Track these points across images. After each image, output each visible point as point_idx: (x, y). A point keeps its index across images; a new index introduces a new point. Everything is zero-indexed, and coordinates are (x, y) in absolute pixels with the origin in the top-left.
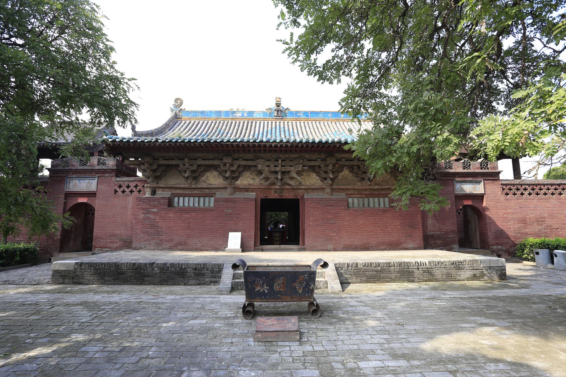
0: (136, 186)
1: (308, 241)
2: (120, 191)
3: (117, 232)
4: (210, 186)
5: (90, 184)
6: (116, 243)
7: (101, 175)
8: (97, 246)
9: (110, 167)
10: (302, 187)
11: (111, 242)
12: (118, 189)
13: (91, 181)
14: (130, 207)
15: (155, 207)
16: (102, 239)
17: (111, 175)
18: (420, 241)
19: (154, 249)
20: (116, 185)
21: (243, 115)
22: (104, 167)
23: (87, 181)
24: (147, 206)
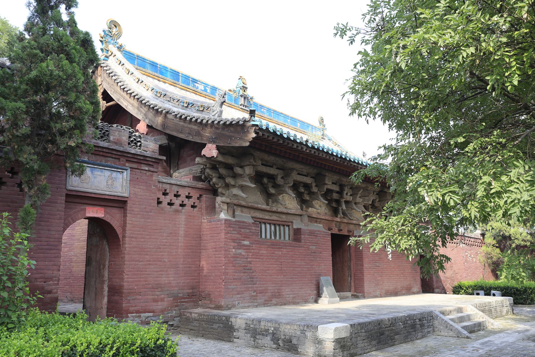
0: (188, 197)
1: (367, 286)
2: (165, 200)
3: (164, 280)
4: (289, 211)
5: (114, 180)
6: (162, 300)
7: (135, 166)
8: (131, 309)
9: (148, 154)
10: (354, 222)
11: (155, 301)
12: (162, 198)
13: (114, 174)
14: (182, 233)
15: (246, 237)
16: (139, 294)
17: (152, 169)
18: (417, 286)
19: (249, 306)
20: (159, 190)
21: (205, 90)
22: (137, 151)
23: (107, 173)
24: (238, 236)
